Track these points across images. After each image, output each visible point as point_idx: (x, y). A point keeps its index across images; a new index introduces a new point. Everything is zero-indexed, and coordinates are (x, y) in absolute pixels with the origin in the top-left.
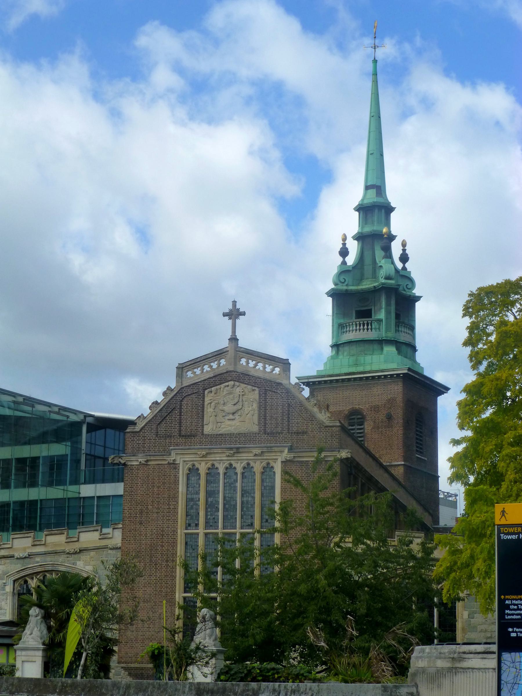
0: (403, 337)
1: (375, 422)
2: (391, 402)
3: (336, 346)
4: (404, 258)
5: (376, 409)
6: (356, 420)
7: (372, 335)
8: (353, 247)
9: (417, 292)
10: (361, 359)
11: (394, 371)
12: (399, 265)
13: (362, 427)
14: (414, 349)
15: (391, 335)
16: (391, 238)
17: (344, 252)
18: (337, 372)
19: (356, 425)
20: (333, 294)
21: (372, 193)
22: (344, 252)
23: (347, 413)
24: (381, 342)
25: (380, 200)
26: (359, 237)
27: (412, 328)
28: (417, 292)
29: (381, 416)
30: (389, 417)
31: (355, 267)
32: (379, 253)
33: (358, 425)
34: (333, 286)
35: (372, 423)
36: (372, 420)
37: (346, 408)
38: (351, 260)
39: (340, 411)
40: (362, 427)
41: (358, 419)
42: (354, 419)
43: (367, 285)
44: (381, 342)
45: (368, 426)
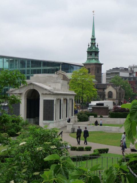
0: (96, 58)
2: (93, 67)
3: (87, 59)
4: (97, 46)
7: (92, 58)
8: (90, 45)
9: (99, 51)
10: (91, 61)
12: (97, 47)
14: (98, 59)
15: (94, 58)
16: (95, 43)
17: (89, 46)
18: (87, 63)
20: (87, 51)
21: (93, 37)
22: (89, 46)
24: (93, 59)
25: (94, 38)
26: (91, 43)
27: (98, 56)
28: (99, 51)
29: (92, 69)
30: (93, 69)
31: (90, 47)
32: (93, 46)
34: (87, 50)
38: (90, 47)
43: (92, 50)
44: (93, 59)
45: (91, 70)
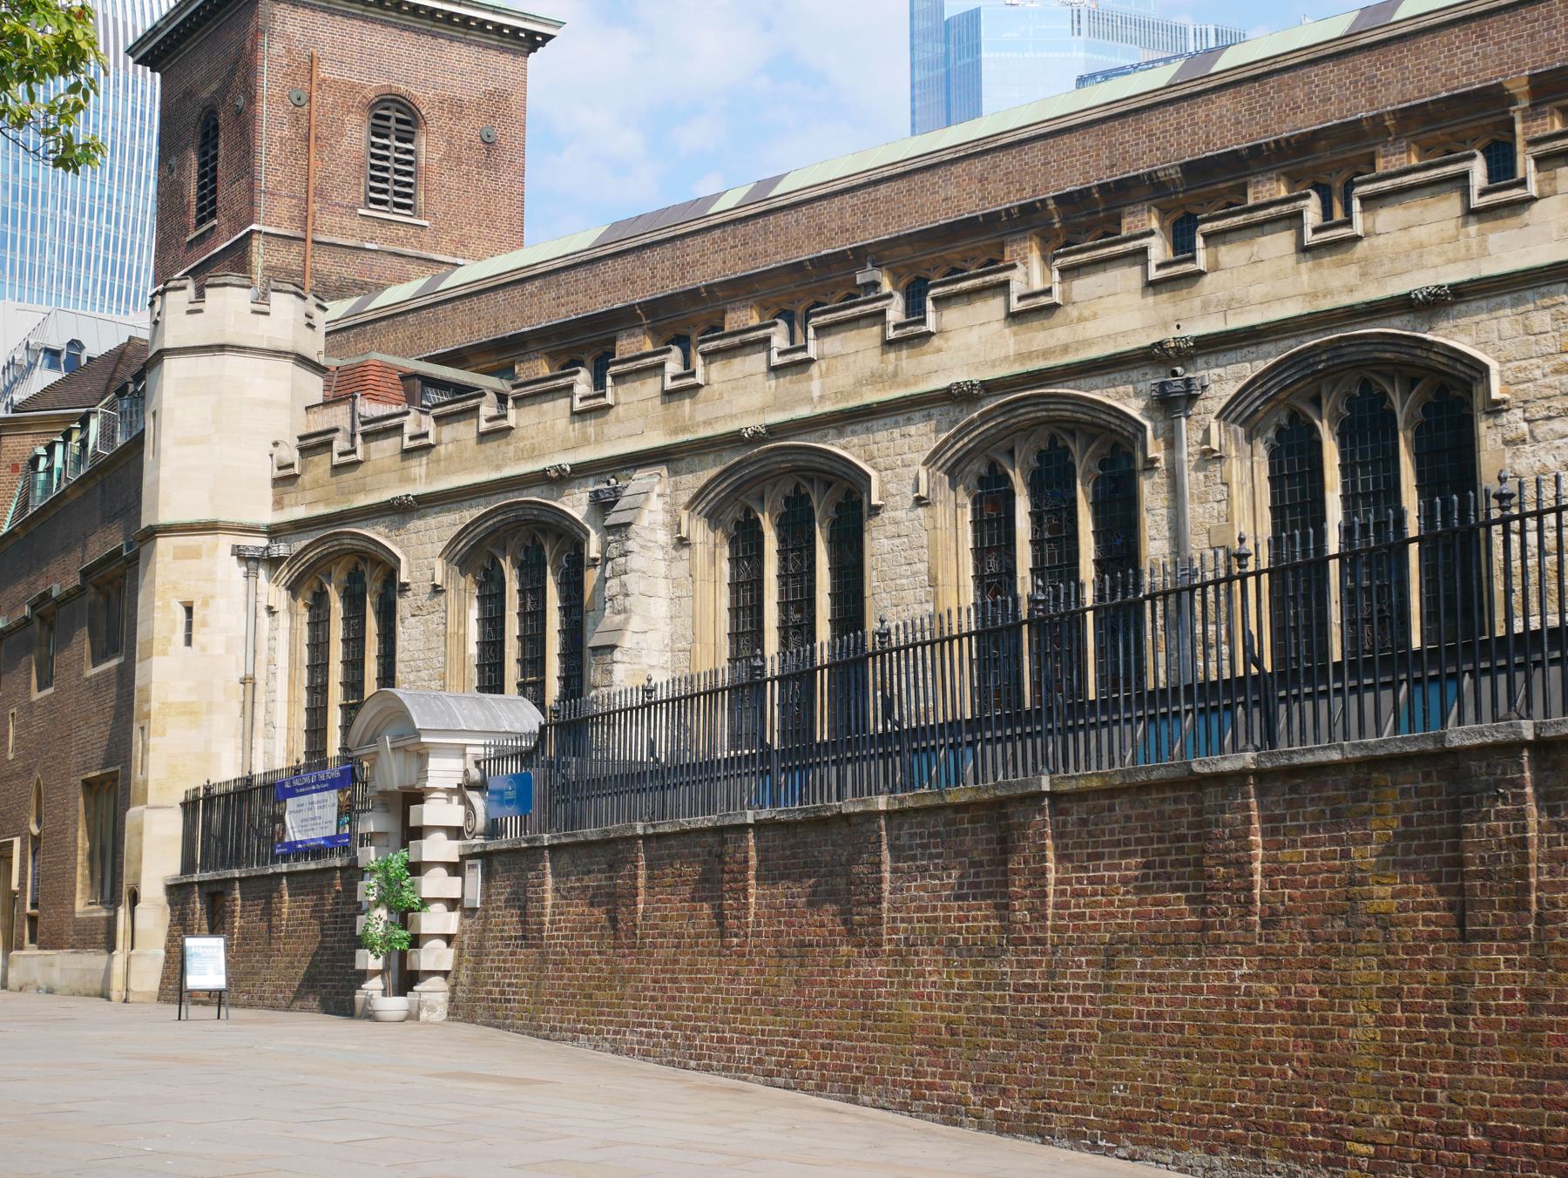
1: (449, 143)
5: (456, 108)
6: (392, 123)
11: (526, 20)
13: (409, 146)
19: (393, 137)
23: (372, 95)
29: (469, 130)
33: (399, 139)
35: (443, 146)
36: (442, 135)
37: (375, 84)
39: (353, 86)
40: (409, 146)
41: (399, 121)
42: (387, 118)
45: (427, 148)
